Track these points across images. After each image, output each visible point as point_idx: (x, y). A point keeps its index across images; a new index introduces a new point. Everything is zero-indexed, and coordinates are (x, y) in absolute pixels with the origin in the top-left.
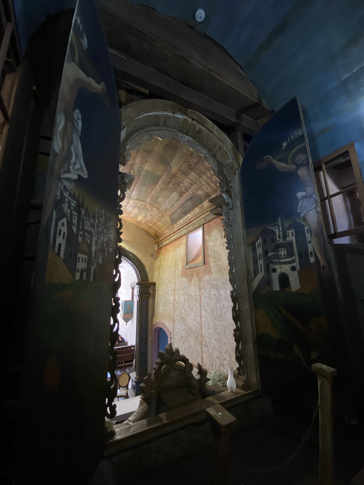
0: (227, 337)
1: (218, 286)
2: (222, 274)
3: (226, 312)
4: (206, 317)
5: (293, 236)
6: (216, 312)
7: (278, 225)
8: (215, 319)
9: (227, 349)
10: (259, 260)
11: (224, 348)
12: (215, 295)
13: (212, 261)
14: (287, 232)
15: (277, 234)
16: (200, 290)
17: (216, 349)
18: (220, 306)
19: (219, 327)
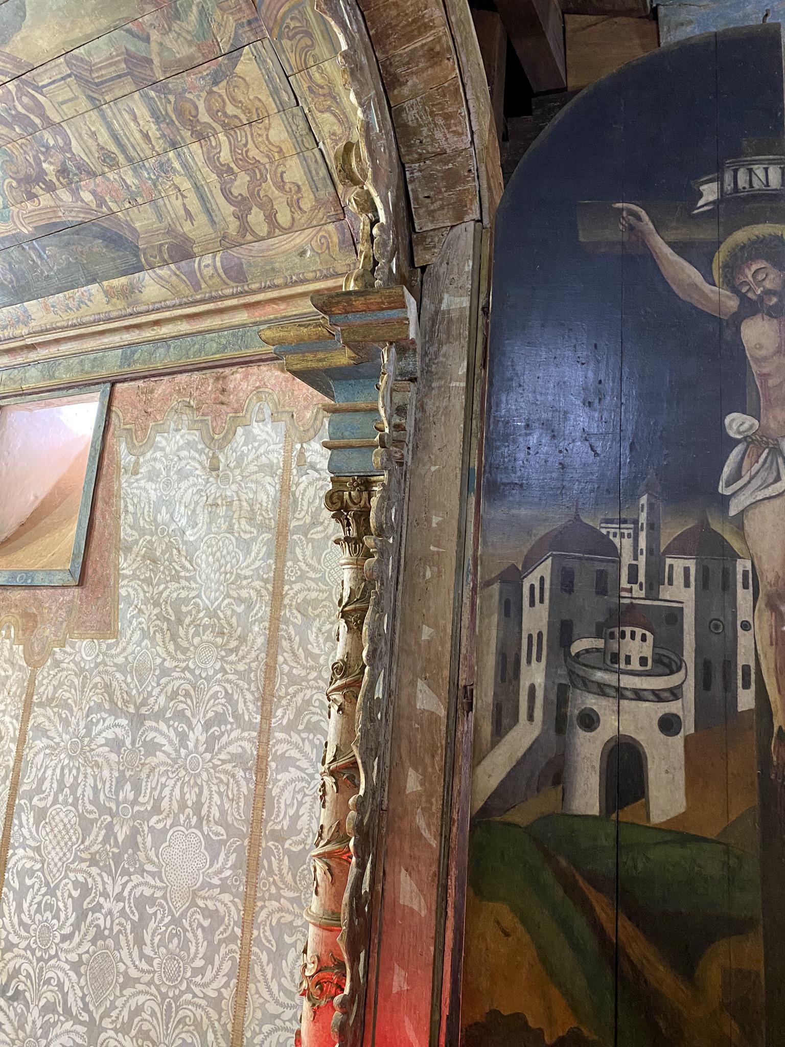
0: (148, 951)
1: (144, 703)
2: (178, 647)
3: (165, 831)
4: (37, 849)
5: (687, 585)
6: (110, 827)
7: (636, 522)
8: (93, 862)
9: (139, 1010)
10: (529, 662)
11: (119, 1003)
12: (116, 745)
13: (134, 577)
14: (669, 561)
15: (627, 559)
16: (28, 706)
17: (67, 1012)
18: (135, 802)
19: (107, 905)
